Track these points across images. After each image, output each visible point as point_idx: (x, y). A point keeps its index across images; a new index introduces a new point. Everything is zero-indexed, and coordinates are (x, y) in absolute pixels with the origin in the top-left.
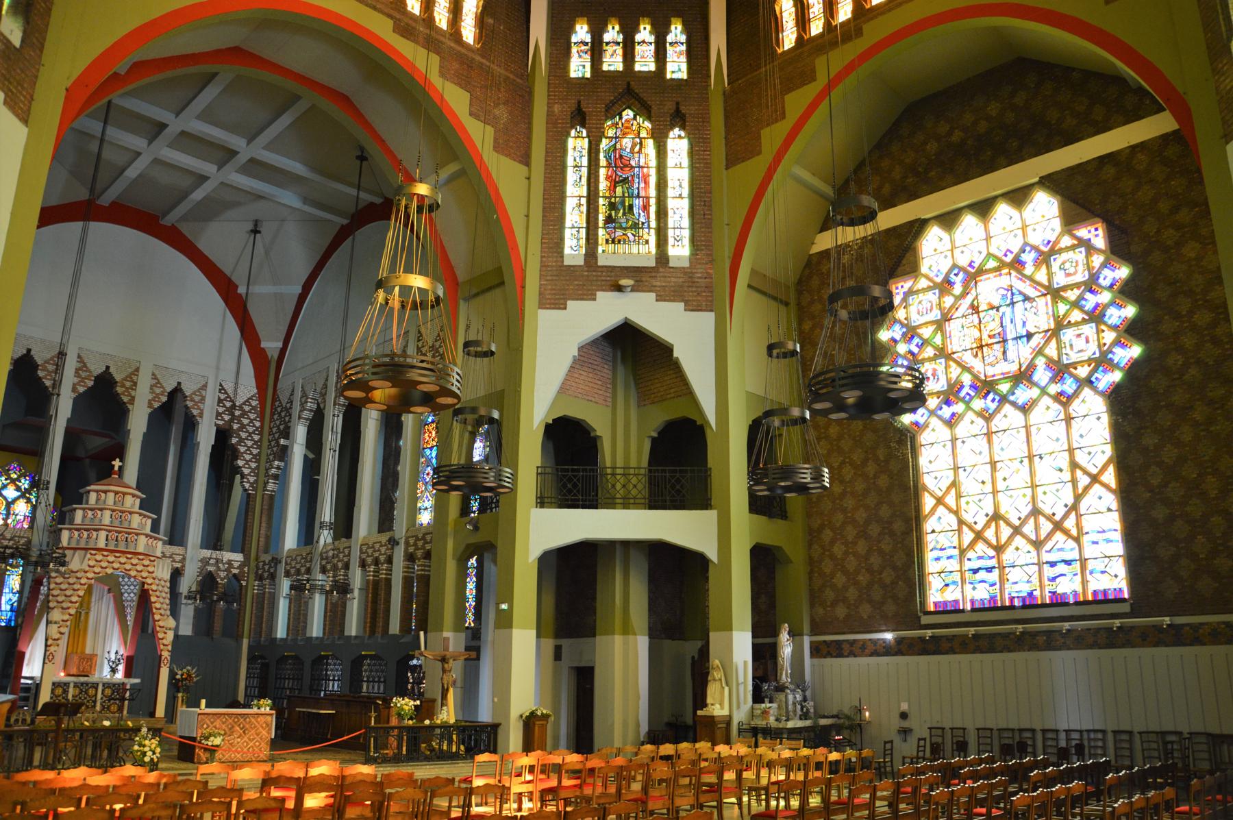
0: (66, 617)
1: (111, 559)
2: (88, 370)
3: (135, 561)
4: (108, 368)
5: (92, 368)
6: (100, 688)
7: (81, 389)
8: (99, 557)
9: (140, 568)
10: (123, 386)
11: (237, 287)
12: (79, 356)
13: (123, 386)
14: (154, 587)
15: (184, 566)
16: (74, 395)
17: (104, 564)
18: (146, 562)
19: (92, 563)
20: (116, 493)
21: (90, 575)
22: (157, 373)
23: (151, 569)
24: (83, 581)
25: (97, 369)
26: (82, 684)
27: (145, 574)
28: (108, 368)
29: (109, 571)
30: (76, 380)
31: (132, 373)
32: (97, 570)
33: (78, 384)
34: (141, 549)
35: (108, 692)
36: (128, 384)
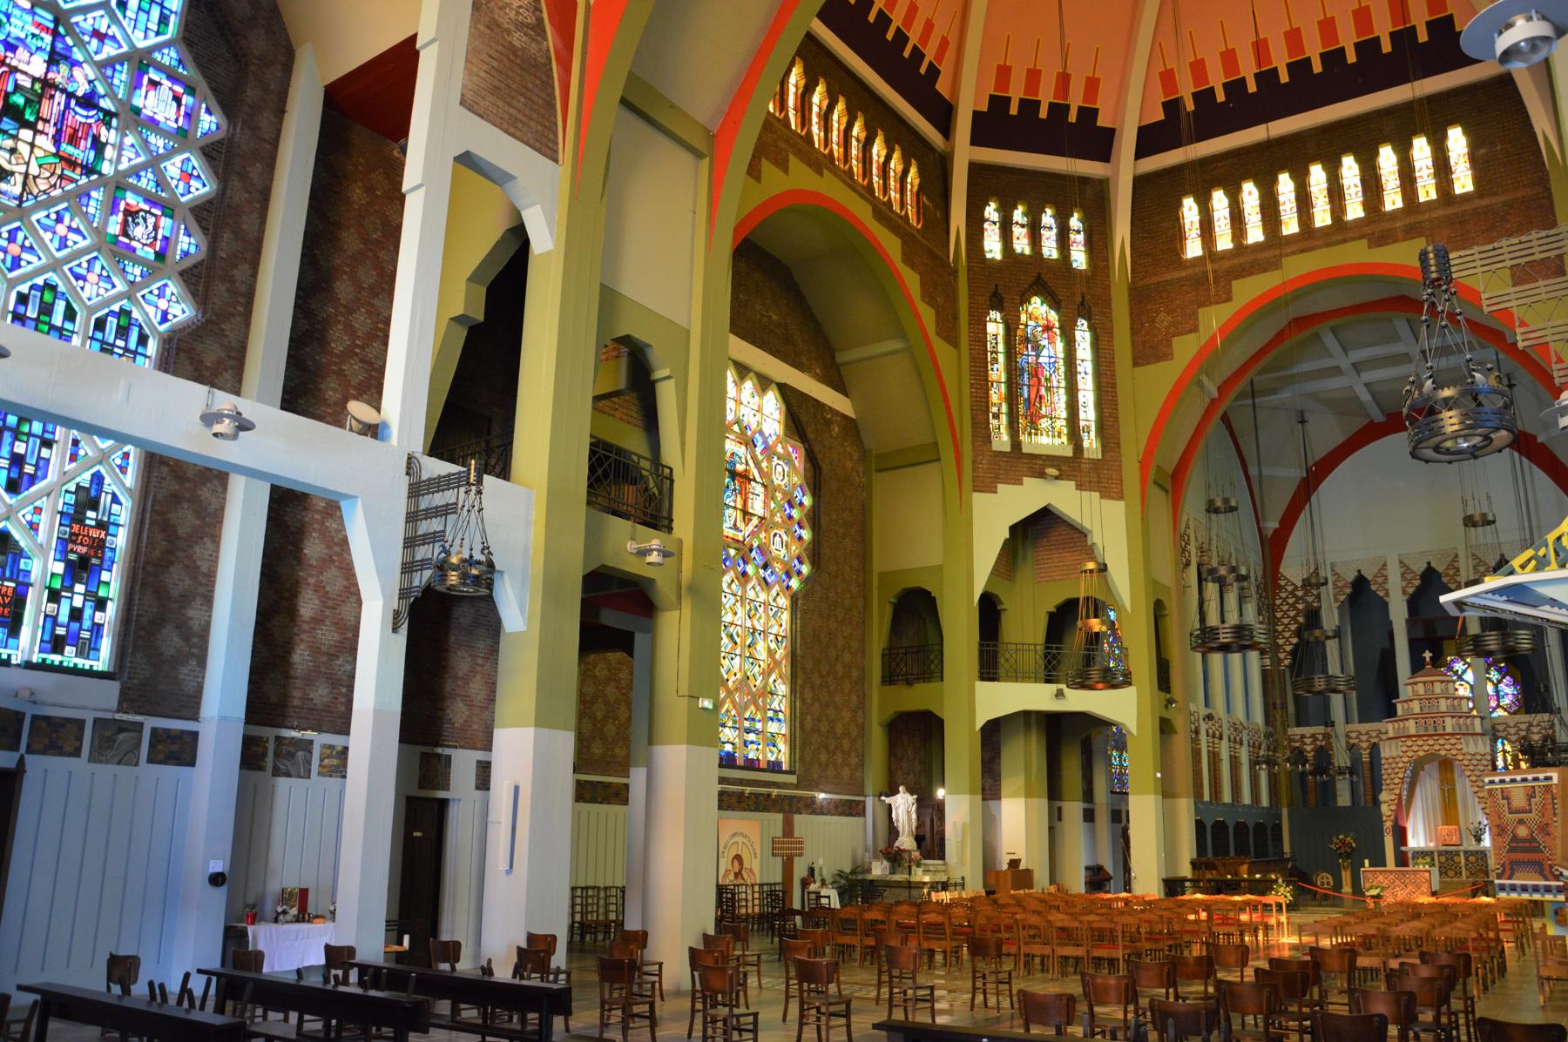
0: (1393, 797)
1: (1420, 743)
2: (1412, 572)
3: (1442, 742)
4: (1429, 563)
5: (1414, 568)
6: (1462, 854)
7: (1411, 590)
8: (1410, 743)
9: (1448, 747)
10: (1447, 575)
11: (1535, 437)
12: (1401, 562)
13: (1447, 575)
14: (1466, 763)
15: (1554, 732)
16: (1406, 598)
17: (1415, 748)
18: (1453, 741)
19: (1405, 749)
20: (1425, 683)
21: (1406, 759)
22: (1476, 552)
23: (1459, 747)
24: (1401, 765)
25: (1420, 568)
26: (1447, 852)
27: (1454, 752)
28: (1429, 563)
29: (1421, 754)
30: (1404, 584)
31: (1453, 561)
32: (1410, 754)
33: (1407, 586)
34: (1449, 730)
35: (1472, 859)
36: (1451, 572)
